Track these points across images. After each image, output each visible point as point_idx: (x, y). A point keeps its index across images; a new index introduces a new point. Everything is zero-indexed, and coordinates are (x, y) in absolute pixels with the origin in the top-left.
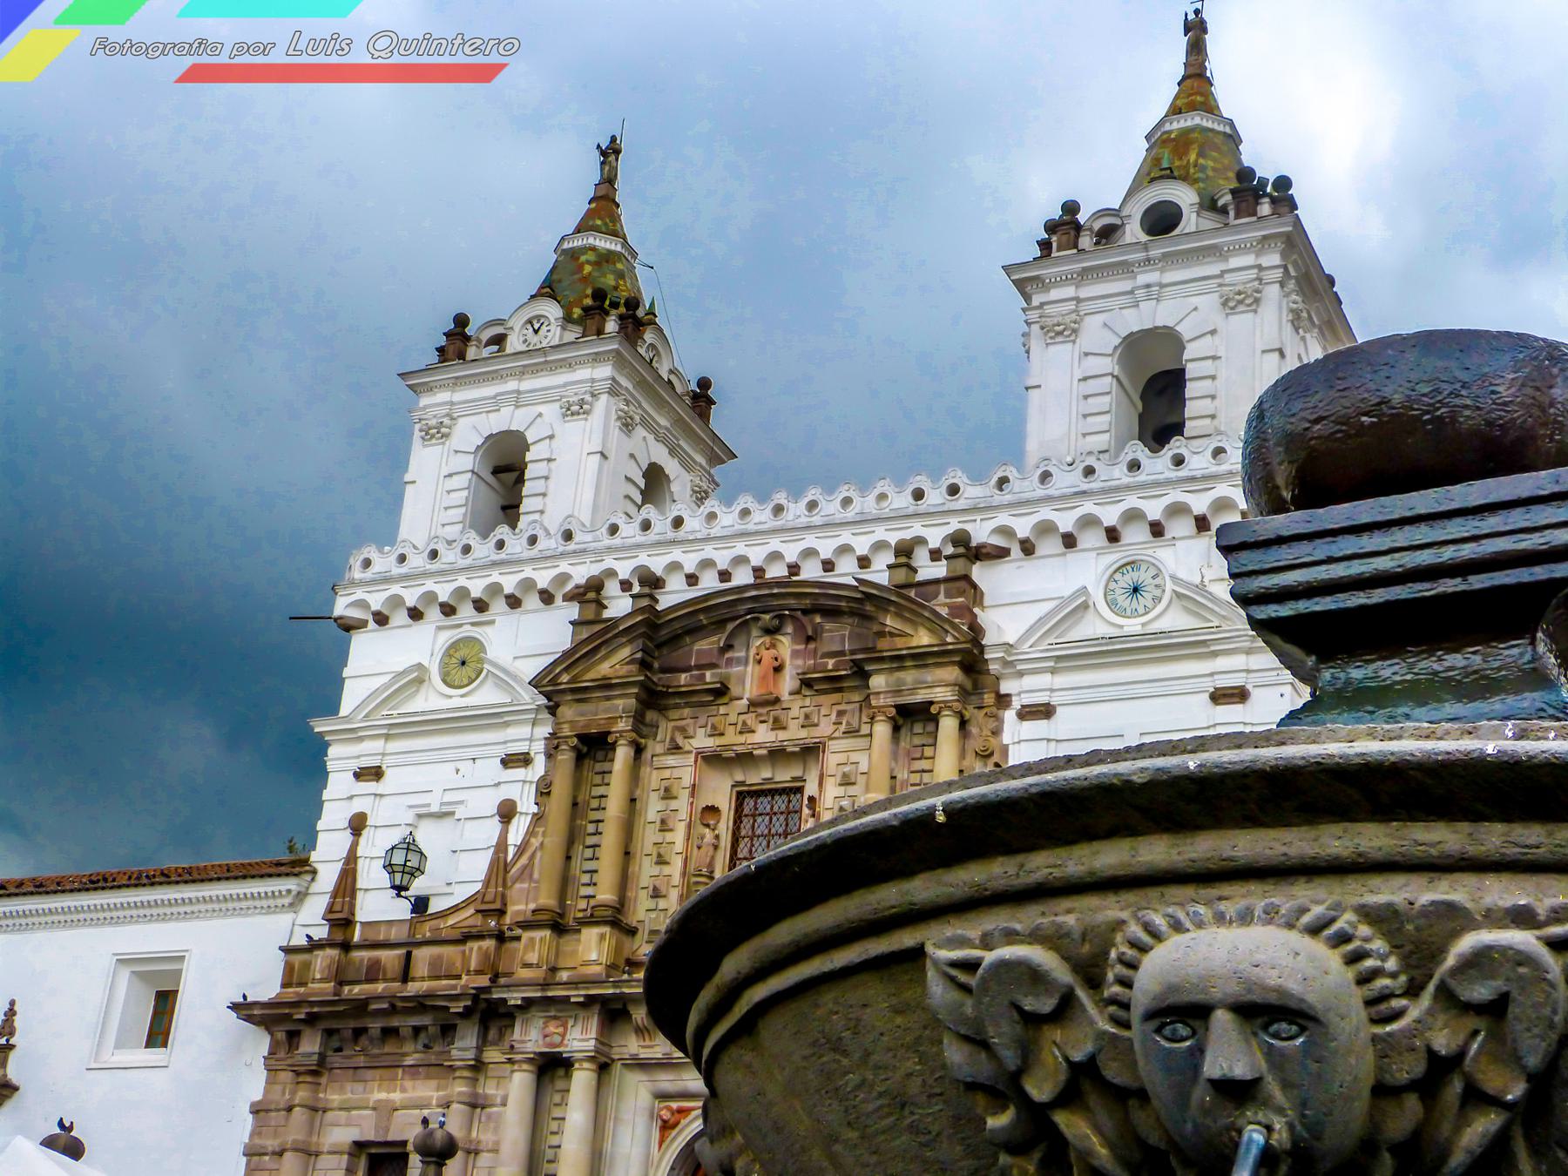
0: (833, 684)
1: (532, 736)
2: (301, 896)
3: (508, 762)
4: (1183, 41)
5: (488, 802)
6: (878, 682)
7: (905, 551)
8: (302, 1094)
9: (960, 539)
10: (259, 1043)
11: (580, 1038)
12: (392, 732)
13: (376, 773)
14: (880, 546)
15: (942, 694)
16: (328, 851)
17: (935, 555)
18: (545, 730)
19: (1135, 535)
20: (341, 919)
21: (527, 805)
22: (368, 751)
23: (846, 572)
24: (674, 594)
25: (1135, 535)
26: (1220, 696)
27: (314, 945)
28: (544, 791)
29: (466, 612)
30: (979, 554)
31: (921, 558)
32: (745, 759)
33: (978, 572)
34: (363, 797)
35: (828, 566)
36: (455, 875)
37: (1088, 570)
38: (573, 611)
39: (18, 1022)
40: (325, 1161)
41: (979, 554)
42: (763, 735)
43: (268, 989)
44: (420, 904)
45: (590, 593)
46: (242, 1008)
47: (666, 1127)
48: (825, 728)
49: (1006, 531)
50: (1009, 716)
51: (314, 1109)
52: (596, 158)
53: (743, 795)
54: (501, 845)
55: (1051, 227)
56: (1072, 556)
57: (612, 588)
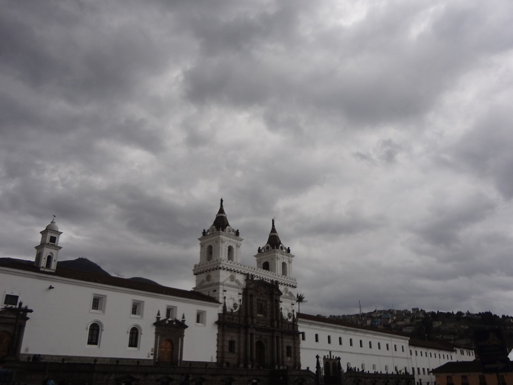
1: (241, 291)
3: (239, 294)
7: (272, 281)
11: (254, 331)
13: (225, 291)
22: (226, 288)
24: (255, 279)
28: (243, 299)
39: (185, 316)
42: (262, 298)
45: (248, 275)
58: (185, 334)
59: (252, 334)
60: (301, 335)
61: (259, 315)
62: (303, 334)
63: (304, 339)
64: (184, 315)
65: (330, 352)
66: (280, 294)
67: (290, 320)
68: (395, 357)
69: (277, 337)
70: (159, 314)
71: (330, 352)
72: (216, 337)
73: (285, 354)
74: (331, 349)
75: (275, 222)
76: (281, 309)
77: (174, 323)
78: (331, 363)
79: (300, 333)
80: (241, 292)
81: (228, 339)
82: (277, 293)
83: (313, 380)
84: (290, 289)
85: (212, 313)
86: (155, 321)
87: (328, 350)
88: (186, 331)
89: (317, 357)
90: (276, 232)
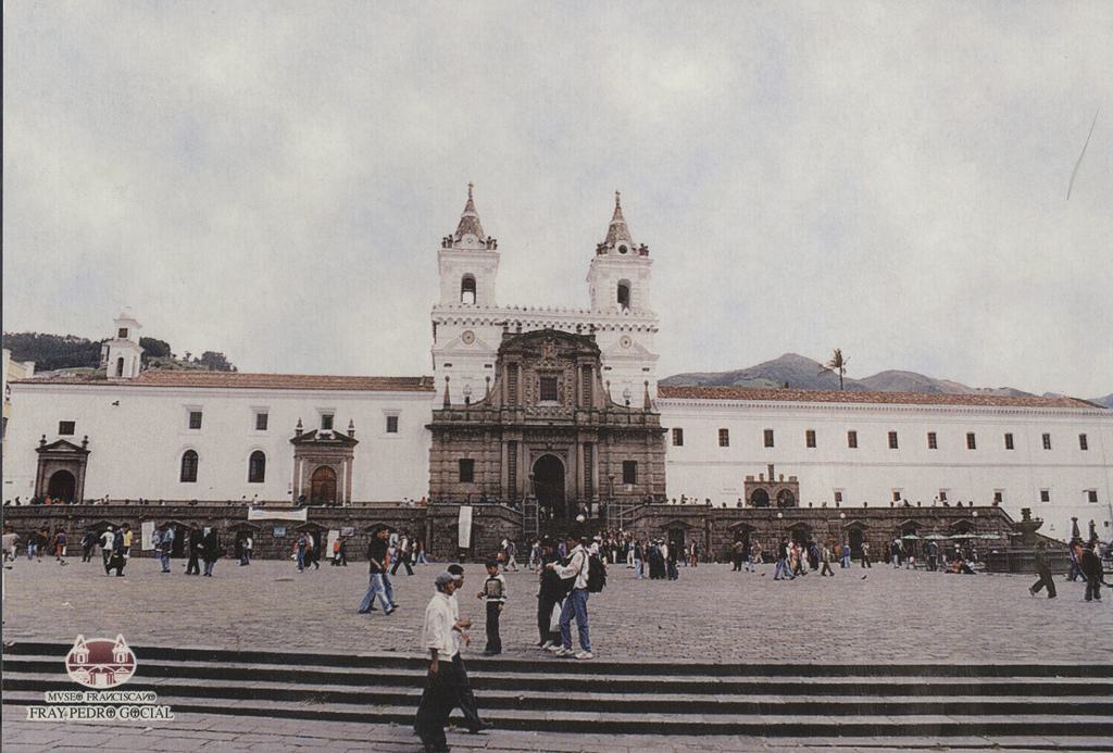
0: (565, 356)
1: (493, 360)
2: (434, 397)
3: (486, 366)
5: (484, 378)
6: (579, 358)
7: (579, 326)
8: (446, 447)
9: (592, 326)
12: (454, 355)
15: (593, 363)
16: (439, 385)
18: (496, 359)
19: (626, 330)
20: (447, 404)
21: (493, 377)
23: (565, 329)
24: (525, 330)
25: (626, 330)
26: (644, 370)
28: (497, 376)
29: (469, 324)
30: (596, 329)
32: (546, 371)
33: (596, 333)
34: (448, 372)
36: (478, 396)
37: (617, 335)
38: (501, 330)
39: (354, 424)
41: (596, 329)
42: (549, 367)
43: (430, 422)
44: (467, 400)
45: (506, 323)
47: (532, 456)
48: (563, 367)
49: (600, 325)
50: (602, 368)
51: (450, 451)
53: (542, 379)
54: (488, 389)
56: (614, 332)
59: (512, 444)
60: (669, 437)
61: (544, 403)
62: (678, 434)
63: (679, 441)
64: (351, 422)
65: (771, 467)
66: (597, 354)
67: (637, 404)
68: (1035, 465)
69: (588, 445)
70: (300, 425)
71: (771, 467)
72: (428, 454)
73: (619, 479)
76: (608, 384)
77: (332, 437)
78: (773, 494)
79: (667, 430)
81: (461, 456)
82: (587, 350)
84: (636, 337)
85: (418, 411)
86: (294, 436)
87: (765, 463)
88: (356, 448)
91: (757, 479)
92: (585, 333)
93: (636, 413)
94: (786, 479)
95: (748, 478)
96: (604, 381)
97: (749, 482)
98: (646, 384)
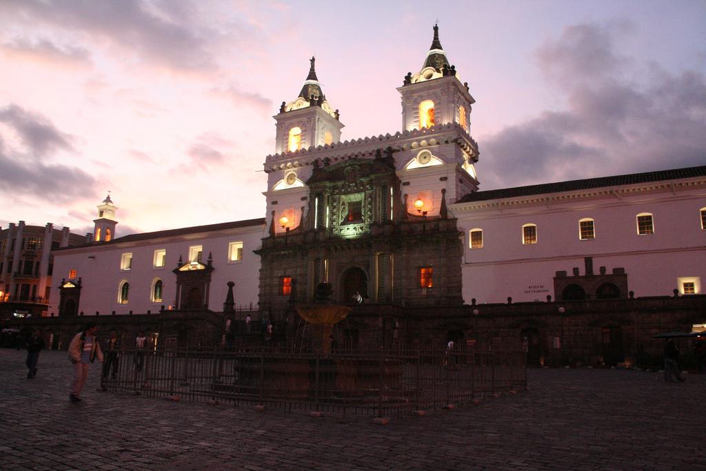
4: (433, 32)
7: (378, 151)
10: (259, 258)
14: (373, 151)
17: (385, 152)
27: (267, 238)
31: (382, 154)
33: (394, 155)
35: (364, 155)
38: (312, 167)
40: (275, 280)
45: (316, 163)
46: (255, 252)
50: (401, 184)
52: (310, 62)
54: (302, 215)
55: (406, 77)
57: (320, 161)
58: (212, 278)
65: (588, 261)
71: (588, 261)
72: (258, 274)
74: (588, 252)
75: (439, 31)
80: (308, 196)
83: (210, 326)
87: (576, 257)
89: (231, 285)
90: (440, 48)
91: (570, 274)
92: (384, 156)
93: (428, 222)
94: (609, 272)
95: (557, 273)
96: (402, 196)
97: (560, 276)
98: (444, 191)
